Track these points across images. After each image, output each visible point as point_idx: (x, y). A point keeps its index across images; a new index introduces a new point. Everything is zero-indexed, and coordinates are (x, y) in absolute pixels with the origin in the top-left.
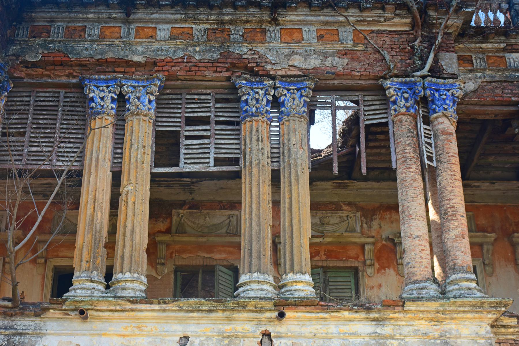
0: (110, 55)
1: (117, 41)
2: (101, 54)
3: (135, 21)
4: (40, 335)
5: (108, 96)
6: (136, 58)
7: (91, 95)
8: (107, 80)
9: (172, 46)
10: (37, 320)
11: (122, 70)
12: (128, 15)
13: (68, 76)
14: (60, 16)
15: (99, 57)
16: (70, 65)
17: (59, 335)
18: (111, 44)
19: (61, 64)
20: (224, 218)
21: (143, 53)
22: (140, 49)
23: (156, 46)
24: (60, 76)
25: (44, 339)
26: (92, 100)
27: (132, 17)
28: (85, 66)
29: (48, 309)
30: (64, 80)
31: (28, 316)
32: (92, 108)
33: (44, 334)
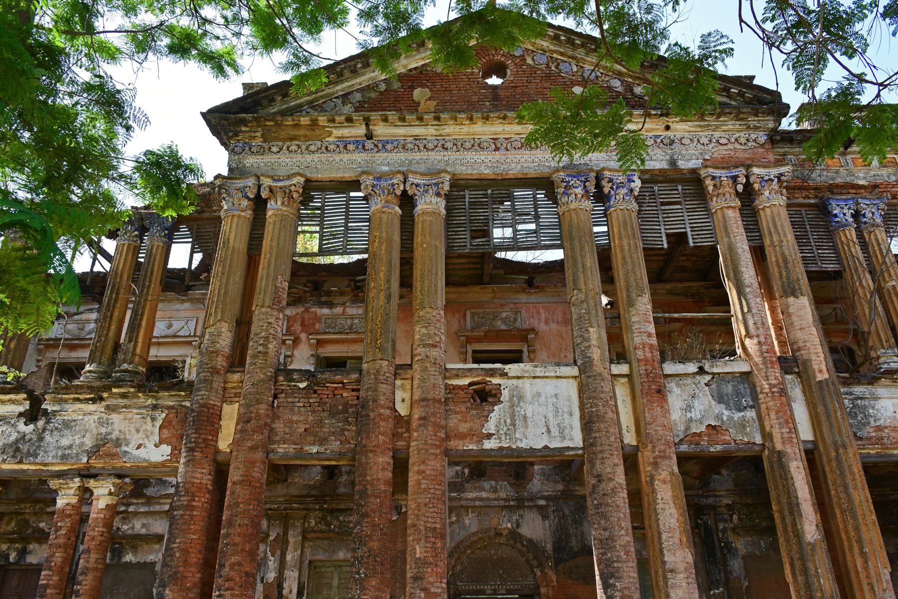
0: (839, 180)
1: (841, 169)
2: (832, 179)
3: (850, 153)
4: (877, 399)
5: (849, 213)
6: (861, 182)
7: (835, 212)
8: (845, 200)
9: (884, 172)
10: (870, 387)
11: (854, 191)
12: (846, 148)
13: (804, 198)
14: (792, 151)
15: (831, 182)
16: (807, 189)
17: (891, 398)
18: (837, 172)
19: (800, 188)
20: (829, 311)
21: (864, 178)
22: (861, 175)
23: (872, 173)
24: (797, 198)
25: (880, 401)
26: (836, 216)
27: (849, 150)
28: (819, 189)
29: (880, 378)
30: (801, 200)
31: (863, 384)
32: (837, 222)
33: (879, 398)
